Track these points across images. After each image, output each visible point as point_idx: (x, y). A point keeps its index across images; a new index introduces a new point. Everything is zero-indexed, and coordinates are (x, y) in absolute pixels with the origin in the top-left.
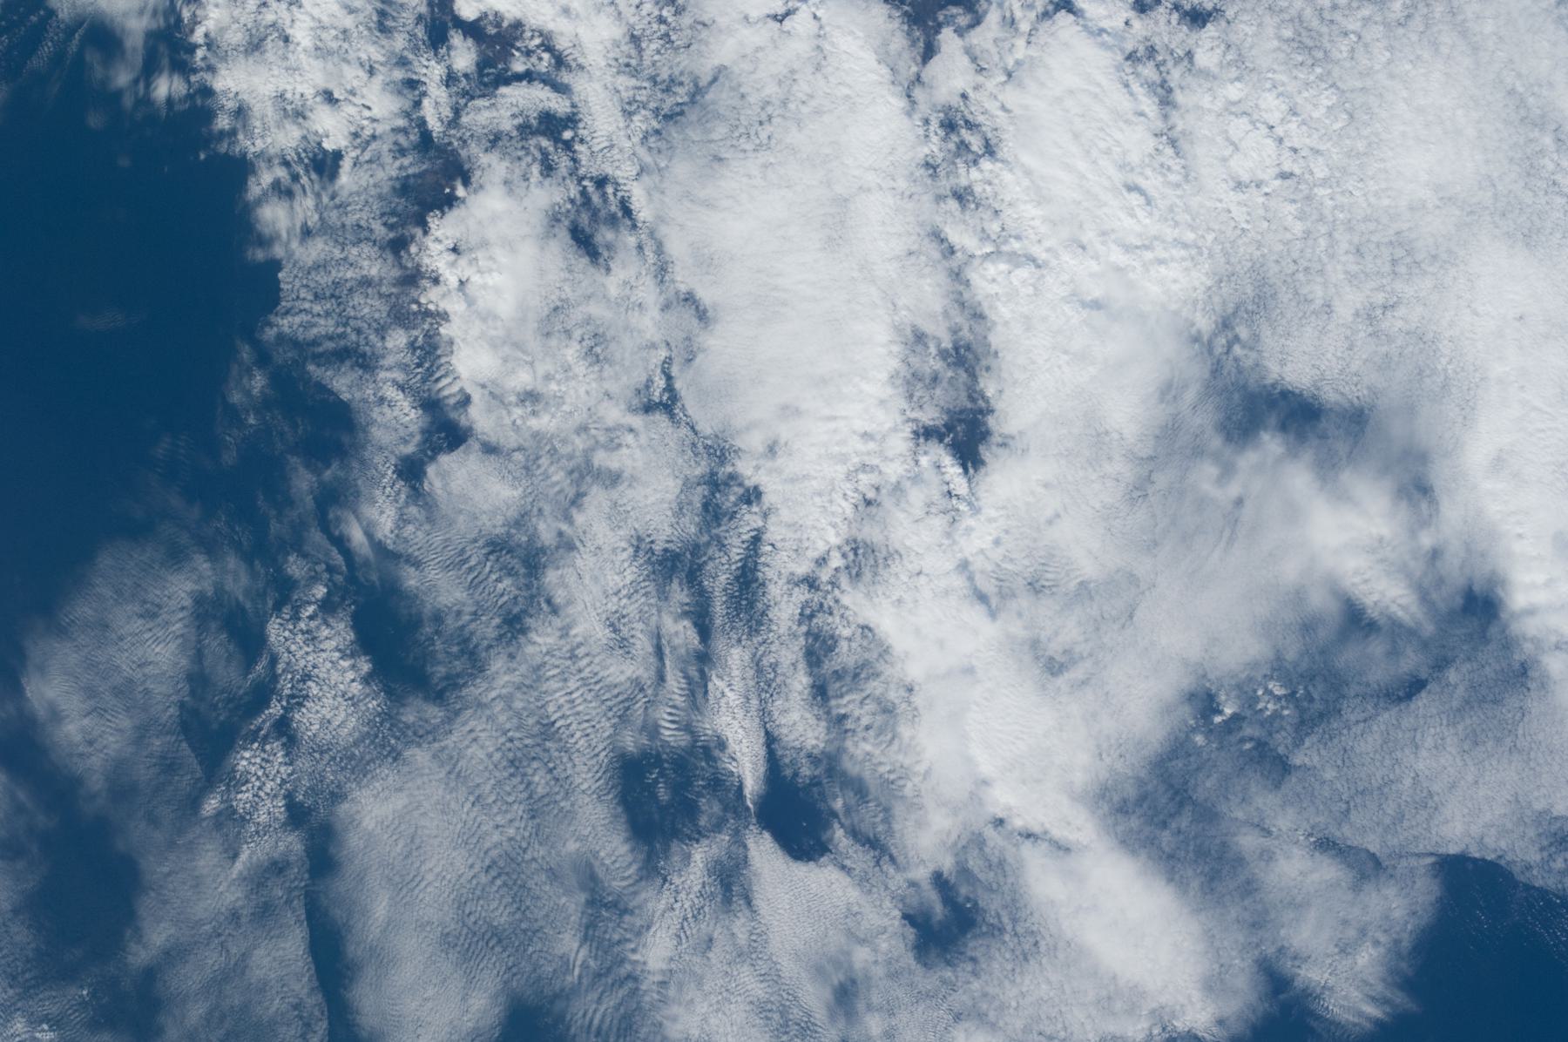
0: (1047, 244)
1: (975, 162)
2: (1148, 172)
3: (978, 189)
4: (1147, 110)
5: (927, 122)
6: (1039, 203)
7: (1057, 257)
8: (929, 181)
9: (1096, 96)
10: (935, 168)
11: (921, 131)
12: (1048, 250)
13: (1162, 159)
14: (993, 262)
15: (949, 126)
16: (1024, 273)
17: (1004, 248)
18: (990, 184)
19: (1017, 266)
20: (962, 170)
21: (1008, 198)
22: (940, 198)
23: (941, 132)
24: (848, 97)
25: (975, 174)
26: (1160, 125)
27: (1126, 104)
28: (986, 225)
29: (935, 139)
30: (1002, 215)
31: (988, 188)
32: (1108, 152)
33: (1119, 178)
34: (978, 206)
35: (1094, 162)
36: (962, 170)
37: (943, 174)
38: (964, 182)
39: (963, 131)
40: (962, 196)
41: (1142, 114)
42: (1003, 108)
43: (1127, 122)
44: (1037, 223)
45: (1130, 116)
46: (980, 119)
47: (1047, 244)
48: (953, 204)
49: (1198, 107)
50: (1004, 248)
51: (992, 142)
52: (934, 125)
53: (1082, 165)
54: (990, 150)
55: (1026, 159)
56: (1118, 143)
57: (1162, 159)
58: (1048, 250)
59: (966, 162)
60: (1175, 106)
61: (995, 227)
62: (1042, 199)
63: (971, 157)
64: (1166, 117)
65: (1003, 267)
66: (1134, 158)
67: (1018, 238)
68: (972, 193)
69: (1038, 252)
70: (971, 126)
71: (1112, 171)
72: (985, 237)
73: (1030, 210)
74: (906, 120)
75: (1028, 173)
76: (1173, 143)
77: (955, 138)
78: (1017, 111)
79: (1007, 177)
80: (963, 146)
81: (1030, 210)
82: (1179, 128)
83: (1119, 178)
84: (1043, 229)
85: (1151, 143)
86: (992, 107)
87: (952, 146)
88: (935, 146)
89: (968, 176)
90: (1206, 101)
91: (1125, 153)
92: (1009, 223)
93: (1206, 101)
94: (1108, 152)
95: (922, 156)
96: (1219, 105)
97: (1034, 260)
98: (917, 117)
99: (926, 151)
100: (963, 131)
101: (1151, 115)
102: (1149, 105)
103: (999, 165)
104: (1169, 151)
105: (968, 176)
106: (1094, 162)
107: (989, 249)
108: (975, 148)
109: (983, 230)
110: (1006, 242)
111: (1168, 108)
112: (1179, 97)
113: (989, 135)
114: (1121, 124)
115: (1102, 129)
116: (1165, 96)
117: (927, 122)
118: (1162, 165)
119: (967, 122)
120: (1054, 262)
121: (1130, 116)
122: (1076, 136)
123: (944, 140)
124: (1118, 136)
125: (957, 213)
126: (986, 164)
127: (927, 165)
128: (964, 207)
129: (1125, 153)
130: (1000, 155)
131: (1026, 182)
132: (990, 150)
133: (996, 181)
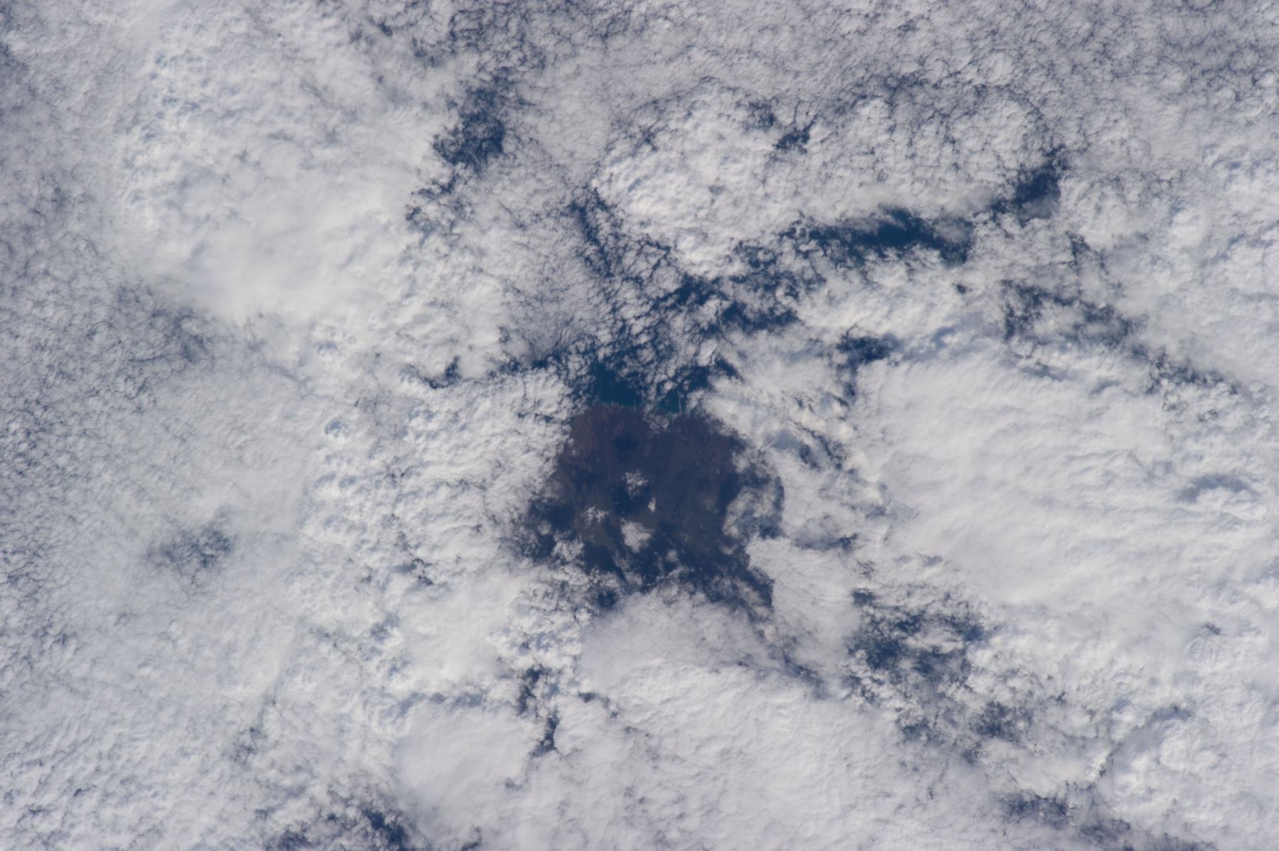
0: (1165, 674)
1: (966, 666)
2: (1192, 446)
3: (1004, 697)
4: (1104, 373)
5: (854, 681)
6: (1097, 636)
7: (1195, 679)
8: (933, 752)
9: (1017, 428)
10: (924, 724)
11: (860, 700)
12: (1176, 681)
13: (1194, 411)
14: (1126, 768)
15: (883, 653)
16: (1175, 744)
17: (1119, 735)
18: (1014, 673)
19: (1158, 740)
20: (961, 695)
21: (1054, 669)
22: (970, 757)
23: (881, 675)
24: (725, 753)
25: (981, 684)
26: (1140, 374)
27: (1062, 397)
28: (1064, 727)
29: (885, 691)
30: (1071, 697)
31: (1015, 683)
32: (1109, 478)
33: (1157, 497)
34: (1028, 717)
35: (1107, 510)
36: (961, 695)
37: (941, 724)
38: (976, 706)
39: (911, 642)
40: (995, 724)
41: (1103, 386)
42: (932, 561)
43: (1094, 416)
44: (1123, 662)
45: (1088, 406)
46: (914, 604)
47: (1165, 674)
48: (996, 748)
49: (1164, 302)
50: (1119, 735)
51: (961, 613)
52: (863, 671)
53: (1096, 530)
54: (972, 633)
55: (1017, 597)
56: (1109, 453)
57: (1194, 411)
58: (1176, 681)
59: (953, 679)
60: (1127, 326)
61: (1077, 721)
62: (1092, 625)
63: (954, 665)
64: (1139, 353)
65: (1141, 763)
66: (1155, 449)
67: (1121, 705)
68: (1003, 710)
69: (1162, 696)
70: (913, 623)
71: (1143, 498)
72: (1078, 744)
73: (1095, 657)
74: (823, 706)
75: (1042, 611)
76: (1187, 375)
77: (906, 664)
78: (943, 551)
79: (1022, 644)
80: (929, 664)
81: (1095, 657)
82: (1173, 348)
83: (1157, 497)
84: (1140, 660)
85: (1153, 408)
86: (913, 573)
87: (915, 677)
88: (894, 702)
89: (981, 688)
90: (1164, 282)
91: (1132, 456)
92: (1085, 697)
93: (1164, 282)
94: (1109, 478)
95: (892, 728)
96: (1187, 268)
97: (1176, 711)
98: (834, 687)
99: (890, 716)
100: (911, 642)
101: (1114, 374)
102: (1097, 364)
103: (996, 640)
104: (1190, 393)
105: (981, 688)
106: (1107, 510)
107: (1100, 759)
108: (947, 647)
109: (1072, 739)
110: (1110, 724)
111: (1130, 340)
112: (1128, 307)
113: (947, 612)
114: (1087, 428)
115: (1072, 458)
116: (1111, 329)
117: (854, 681)
118: (1201, 419)
119: (902, 626)
120: (1198, 691)
121: (1088, 406)
122: (1048, 502)
123: (897, 678)
124: (1098, 445)
125: (1014, 752)
126: (980, 656)
127: (910, 732)
128: (1013, 738)
129: (1132, 456)
130: (986, 625)
131: (1052, 627)
132: (972, 633)
133: (1018, 662)
